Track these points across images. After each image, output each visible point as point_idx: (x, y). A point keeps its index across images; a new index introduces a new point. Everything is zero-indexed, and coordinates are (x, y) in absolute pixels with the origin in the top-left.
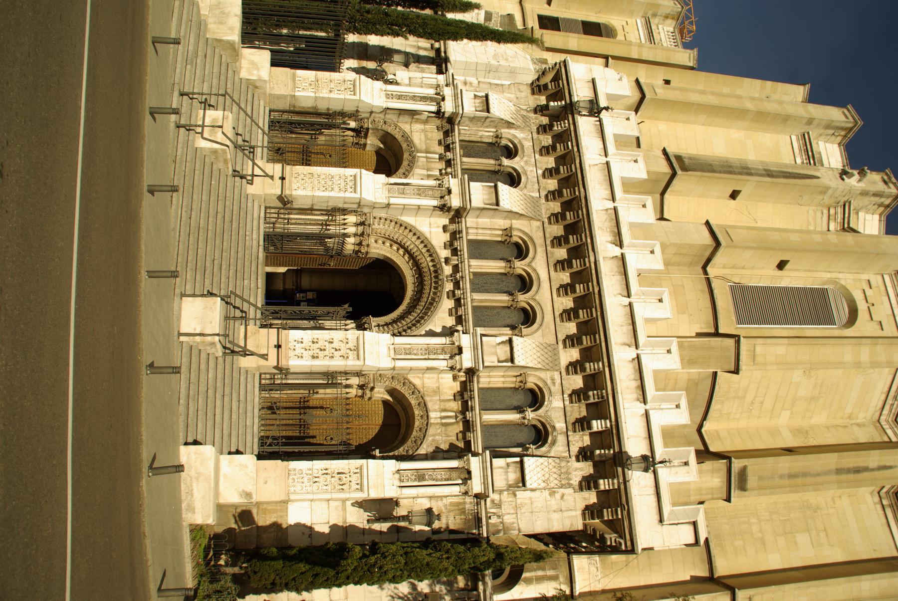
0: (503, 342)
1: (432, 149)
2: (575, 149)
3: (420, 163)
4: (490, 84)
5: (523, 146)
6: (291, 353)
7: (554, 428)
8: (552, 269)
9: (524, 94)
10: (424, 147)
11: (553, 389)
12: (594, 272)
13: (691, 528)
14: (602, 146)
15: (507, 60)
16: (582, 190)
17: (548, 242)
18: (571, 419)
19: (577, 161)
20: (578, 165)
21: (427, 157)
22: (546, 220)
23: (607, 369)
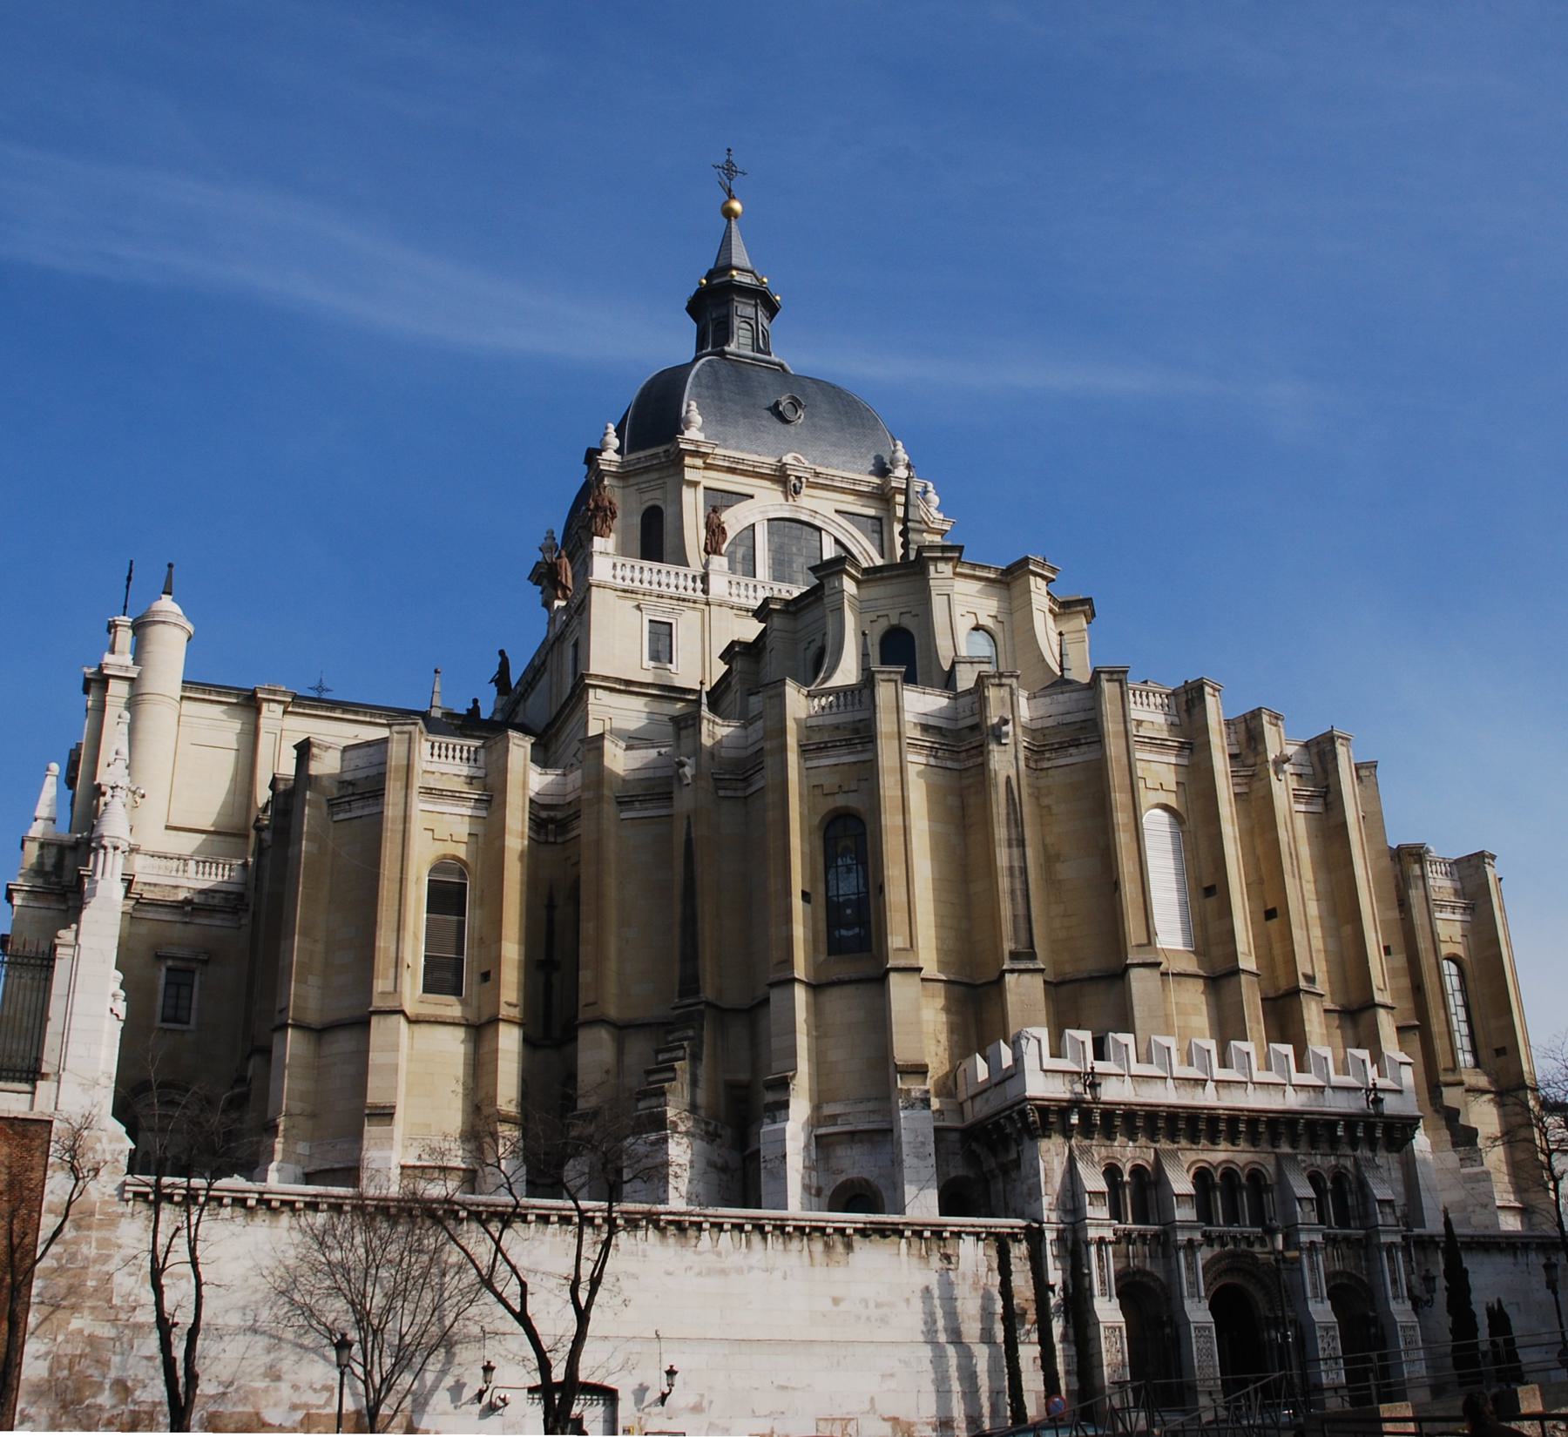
0: (1300, 1206)
1: (1124, 1251)
2: (1122, 1107)
3: (1140, 1265)
4: (1046, 1183)
5: (1108, 1157)
6: (1336, 1381)
7: (1336, 1166)
8: (1217, 1147)
9: (1052, 1147)
10: (1123, 1260)
11: (1308, 1162)
12: (1232, 1112)
13: (1403, 1066)
14: (1114, 1078)
15: (923, 1143)
16: (1161, 1109)
17: (1194, 1147)
18: (1329, 1151)
19: (1134, 1107)
20: (1138, 1108)
21: (1134, 1258)
22: (1176, 1146)
23: (1306, 1116)
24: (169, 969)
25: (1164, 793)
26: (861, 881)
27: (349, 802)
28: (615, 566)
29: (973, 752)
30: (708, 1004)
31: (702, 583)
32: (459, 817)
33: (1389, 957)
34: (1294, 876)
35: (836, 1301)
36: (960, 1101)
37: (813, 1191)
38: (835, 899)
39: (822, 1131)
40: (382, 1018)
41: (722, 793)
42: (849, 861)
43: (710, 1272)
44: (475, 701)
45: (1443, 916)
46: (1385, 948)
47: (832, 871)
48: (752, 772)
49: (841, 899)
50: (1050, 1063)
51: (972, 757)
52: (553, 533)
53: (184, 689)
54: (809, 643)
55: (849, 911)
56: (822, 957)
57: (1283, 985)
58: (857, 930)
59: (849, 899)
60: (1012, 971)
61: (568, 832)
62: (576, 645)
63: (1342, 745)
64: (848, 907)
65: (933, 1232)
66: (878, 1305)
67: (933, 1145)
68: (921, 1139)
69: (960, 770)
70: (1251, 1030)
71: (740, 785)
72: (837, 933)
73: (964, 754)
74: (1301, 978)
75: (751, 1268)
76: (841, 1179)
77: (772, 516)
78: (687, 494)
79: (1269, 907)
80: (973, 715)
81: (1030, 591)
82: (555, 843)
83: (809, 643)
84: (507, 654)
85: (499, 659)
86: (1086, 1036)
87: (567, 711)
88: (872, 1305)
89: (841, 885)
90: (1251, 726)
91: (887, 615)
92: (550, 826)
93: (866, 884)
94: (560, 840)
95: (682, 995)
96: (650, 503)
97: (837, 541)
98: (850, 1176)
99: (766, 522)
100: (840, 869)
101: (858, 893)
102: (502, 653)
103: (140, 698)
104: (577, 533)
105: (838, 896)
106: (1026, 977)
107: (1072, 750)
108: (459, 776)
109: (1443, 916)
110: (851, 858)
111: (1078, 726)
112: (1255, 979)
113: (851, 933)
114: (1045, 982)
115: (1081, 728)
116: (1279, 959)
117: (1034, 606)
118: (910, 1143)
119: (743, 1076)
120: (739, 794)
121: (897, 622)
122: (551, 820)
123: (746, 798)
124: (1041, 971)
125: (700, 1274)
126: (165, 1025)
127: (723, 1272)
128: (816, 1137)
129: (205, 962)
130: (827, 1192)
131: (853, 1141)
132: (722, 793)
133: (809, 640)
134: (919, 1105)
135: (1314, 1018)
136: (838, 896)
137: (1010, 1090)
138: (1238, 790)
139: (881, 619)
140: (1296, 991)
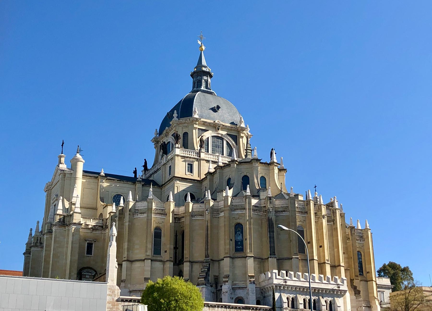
24: (87, 243)
25: (301, 222)
26: (242, 237)
27: (137, 214)
29: (264, 212)
30: (211, 260)
31: (199, 154)
32: (160, 218)
33: (344, 255)
36: (260, 282)
37: (232, 298)
38: (237, 240)
39: (233, 287)
40: (147, 260)
41: (214, 216)
42: (239, 233)
44: (136, 168)
46: (343, 253)
47: (236, 234)
48: (220, 212)
49: (238, 240)
50: (278, 277)
51: (264, 213)
52: (157, 130)
53: (82, 176)
54: (226, 176)
55: (239, 243)
56: (234, 252)
57: (322, 262)
58: (241, 247)
59: (239, 241)
60: (271, 258)
61: (180, 220)
62: (170, 167)
63: (338, 211)
64: (239, 242)
65: (256, 308)
67: (255, 291)
68: (253, 290)
69: (262, 215)
71: (218, 215)
72: (237, 247)
73: (262, 212)
74: (326, 260)
76: (237, 296)
77: (213, 135)
78: (194, 131)
79: (320, 245)
80: (264, 204)
81: (274, 169)
82: (177, 222)
83: (226, 176)
84: (146, 160)
85: (144, 161)
86: (284, 272)
87: (168, 183)
89: (238, 238)
90: (319, 207)
91: (244, 173)
92: (176, 219)
93: (243, 238)
94: (178, 222)
95: (206, 257)
96: (185, 131)
97: (227, 141)
98: (239, 296)
99: (211, 137)
100: (238, 234)
101: (241, 240)
102: (145, 160)
103: (76, 178)
104: (165, 133)
105: (237, 240)
108: (160, 209)
110: (240, 232)
111: (285, 208)
112: (317, 261)
113: (239, 247)
114: (277, 259)
115: (286, 208)
116: (322, 256)
117: (275, 173)
118: (251, 290)
119: (217, 274)
120: (217, 216)
121: (246, 174)
122: (177, 218)
123: (218, 217)
124: (276, 258)
126: (87, 255)
128: (232, 288)
129: (95, 241)
130: (234, 299)
131: (239, 289)
132: (214, 216)
133: (226, 176)
134: (253, 283)
135: (328, 268)
136: (237, 240)
137: (270, 281)
138: (316, 220)
139: (242, 173)
140: (325, 263)
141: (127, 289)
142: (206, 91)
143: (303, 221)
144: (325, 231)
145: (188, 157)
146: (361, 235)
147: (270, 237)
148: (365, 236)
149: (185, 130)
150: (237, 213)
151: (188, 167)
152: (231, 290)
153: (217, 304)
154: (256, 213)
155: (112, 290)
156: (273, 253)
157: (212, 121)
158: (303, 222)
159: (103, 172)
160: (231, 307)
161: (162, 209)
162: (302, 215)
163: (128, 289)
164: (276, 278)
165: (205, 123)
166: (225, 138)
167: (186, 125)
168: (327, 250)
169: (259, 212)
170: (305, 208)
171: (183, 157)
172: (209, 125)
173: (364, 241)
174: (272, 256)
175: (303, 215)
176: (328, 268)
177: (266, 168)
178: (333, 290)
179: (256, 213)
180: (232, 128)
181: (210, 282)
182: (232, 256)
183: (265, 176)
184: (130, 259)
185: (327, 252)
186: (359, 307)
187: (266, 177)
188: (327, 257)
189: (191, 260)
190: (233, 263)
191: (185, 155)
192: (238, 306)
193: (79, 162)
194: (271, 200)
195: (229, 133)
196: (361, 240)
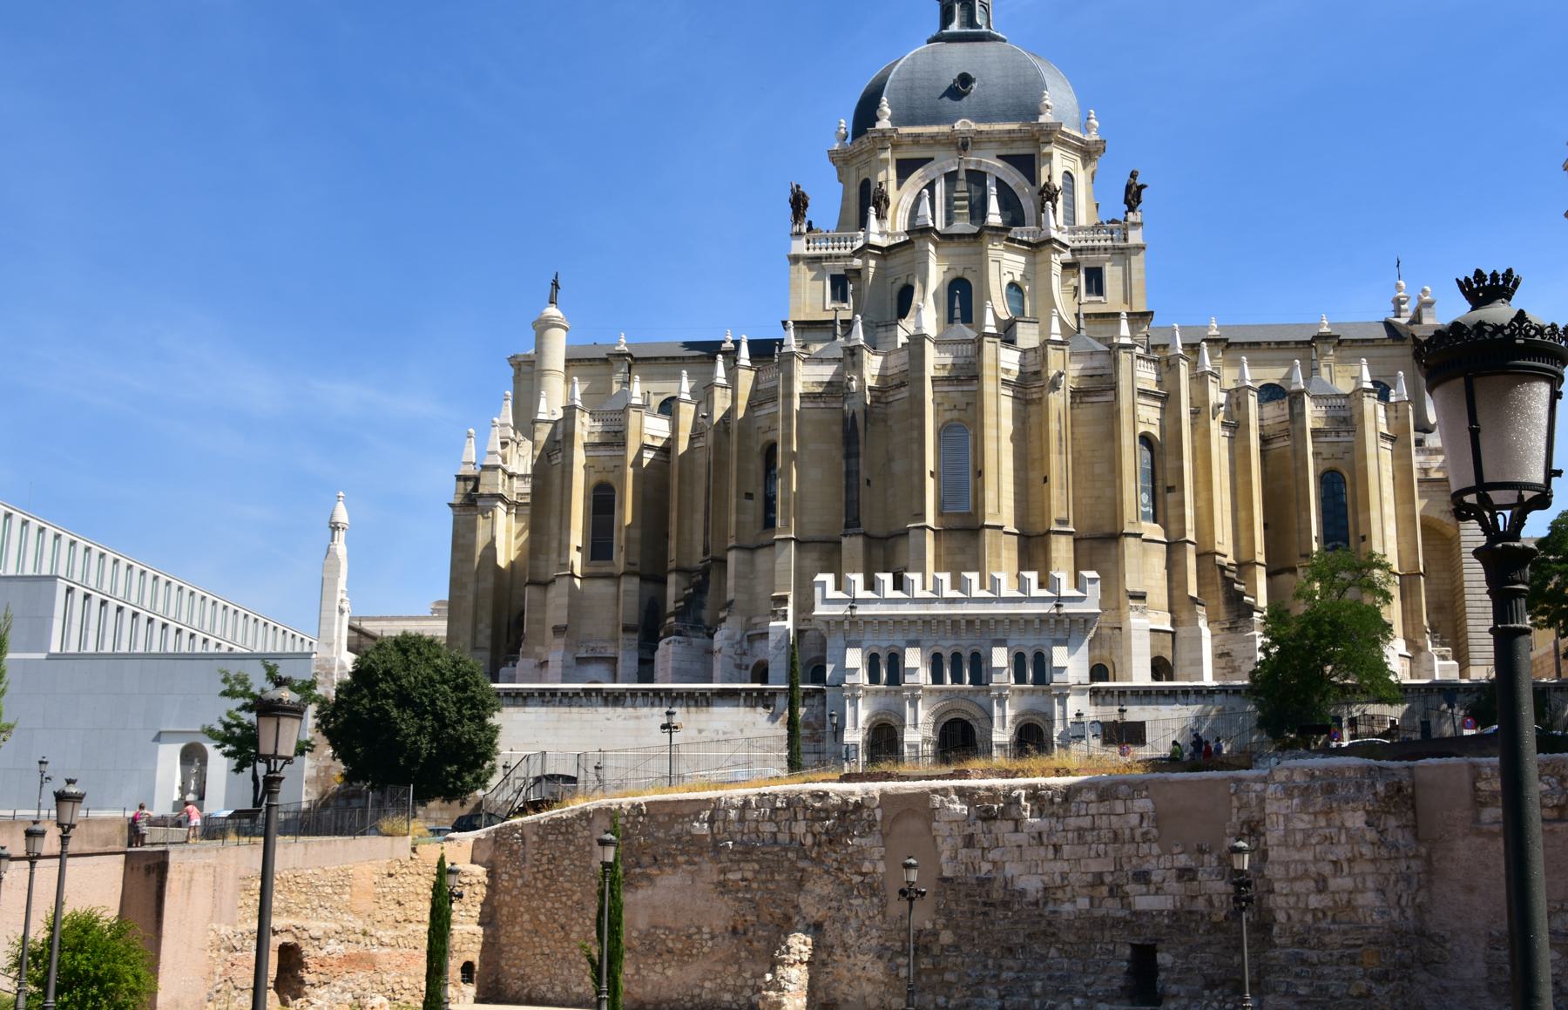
28: (808, 242)
34: (1060, 453)
35: (700, 731)
39: (750, 633)
43: (631, 718)
45: (1328, 439)
60: (845, 535)
66: (724, 733)
70: (989, 562)
75: (653, 715)
76: (757, 660)
88: (720, 732)
106: (853, 539)
107: (902, 389)
108: (608, 432)
109: (1328, 439)
125: (625, 719)
127: (638, 718)
135: (1062, 551)
141: (532, 660)
142: (967, 34)
143: (964, 407)
144: (1054, 426)
145: (829, 257)
146: (1342, 414)
147: (848, 474)
148: (1356, 417)
149: (864, 174)
150: (766, 412)
151: (833, 288)
152: (740, 642)
153: (627, 689)
154: (822, 405)
155: (325, 669)
156: (852, 522)
157: (945, 129)
158: (965, 410)
159: (623, 341)
160: (674, 694)
161: (616, 429)
162: (960, 388)
163: (536, 658)
164: (826, 601)
165: (916, 139)
166: (993, 172)
167: (865, 156)
168: (1062, 488)
169: (833, 399)
170: (974, 364)
171: (814, 261)
172: (931, 142)
173: (1352, 434)
174: (850, 531)
175: (965, 388)
176: (1062, 551)
177: (969, 250)
178: (1043, 619)
179: (822, 405)
180: (1012, 135)
181: (707, 623)
182: (748, 542)
183: (966, 277)
184: (542, 578)
185: (1062, 494)
186: (1246, 661)
187: (970, 279)
188: (1062, 509)
189: (686, 564)
190: (752, 563)
191: (818, 252)
192: (696, 689)
193: (554, 329)
194: (855, 358)
195: (1003, 152)
196: (1338, 432)
